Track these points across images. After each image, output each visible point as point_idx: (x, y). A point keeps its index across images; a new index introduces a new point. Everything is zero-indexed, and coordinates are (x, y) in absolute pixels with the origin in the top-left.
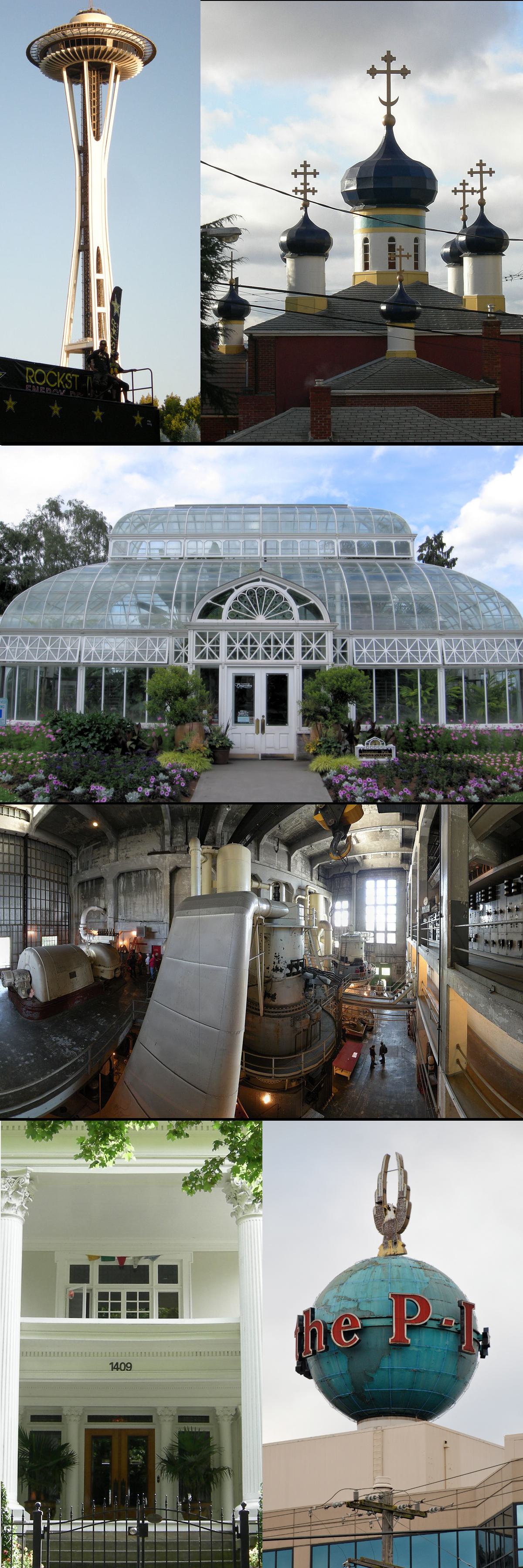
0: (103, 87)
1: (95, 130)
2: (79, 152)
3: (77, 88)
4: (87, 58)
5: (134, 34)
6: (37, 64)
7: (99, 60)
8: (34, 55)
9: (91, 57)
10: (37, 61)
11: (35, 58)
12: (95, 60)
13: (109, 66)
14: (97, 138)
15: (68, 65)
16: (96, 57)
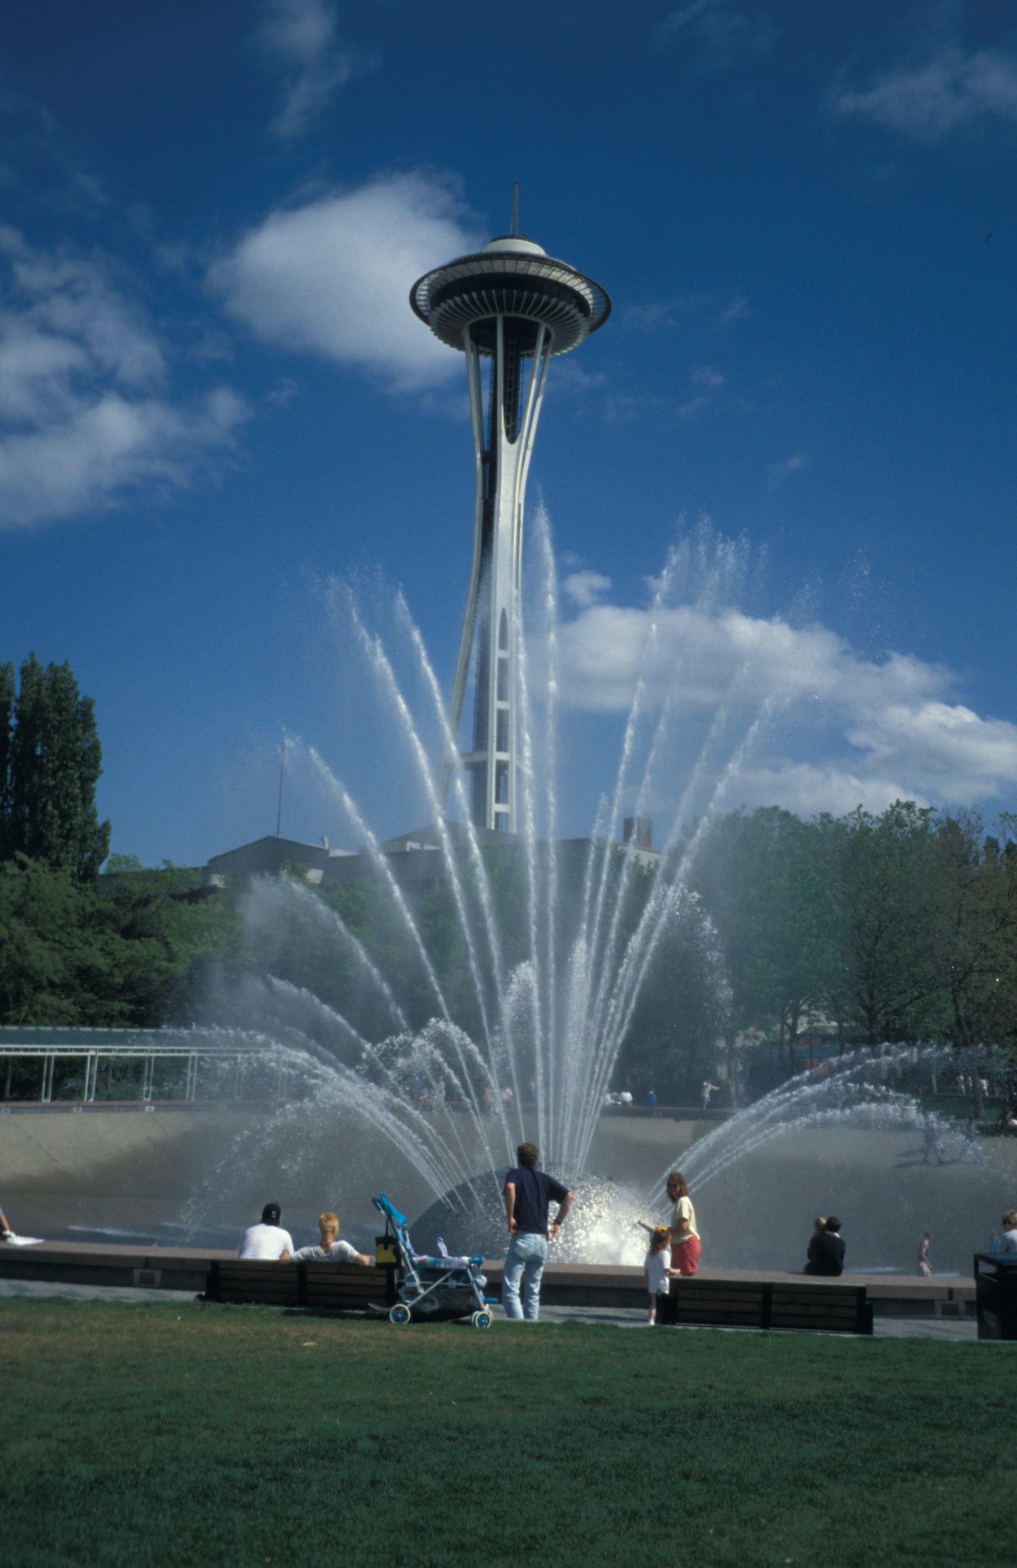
0: (524, 362)
1: (510, 426)
2: (484, 460)
3: (486, 361)
4: (502, 310)
5: (577, 275)
6: (425, 319)
7: (519, 315)
8: (423, 303)
9: (509, 310)
10: (426, 314)
11: (423, 308)
12: (513, 314)
13: (536, 326)
14: (512, 440)
15: (472, 321)
16: (516, 310)
